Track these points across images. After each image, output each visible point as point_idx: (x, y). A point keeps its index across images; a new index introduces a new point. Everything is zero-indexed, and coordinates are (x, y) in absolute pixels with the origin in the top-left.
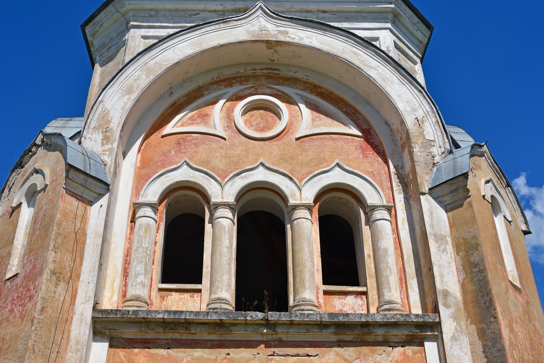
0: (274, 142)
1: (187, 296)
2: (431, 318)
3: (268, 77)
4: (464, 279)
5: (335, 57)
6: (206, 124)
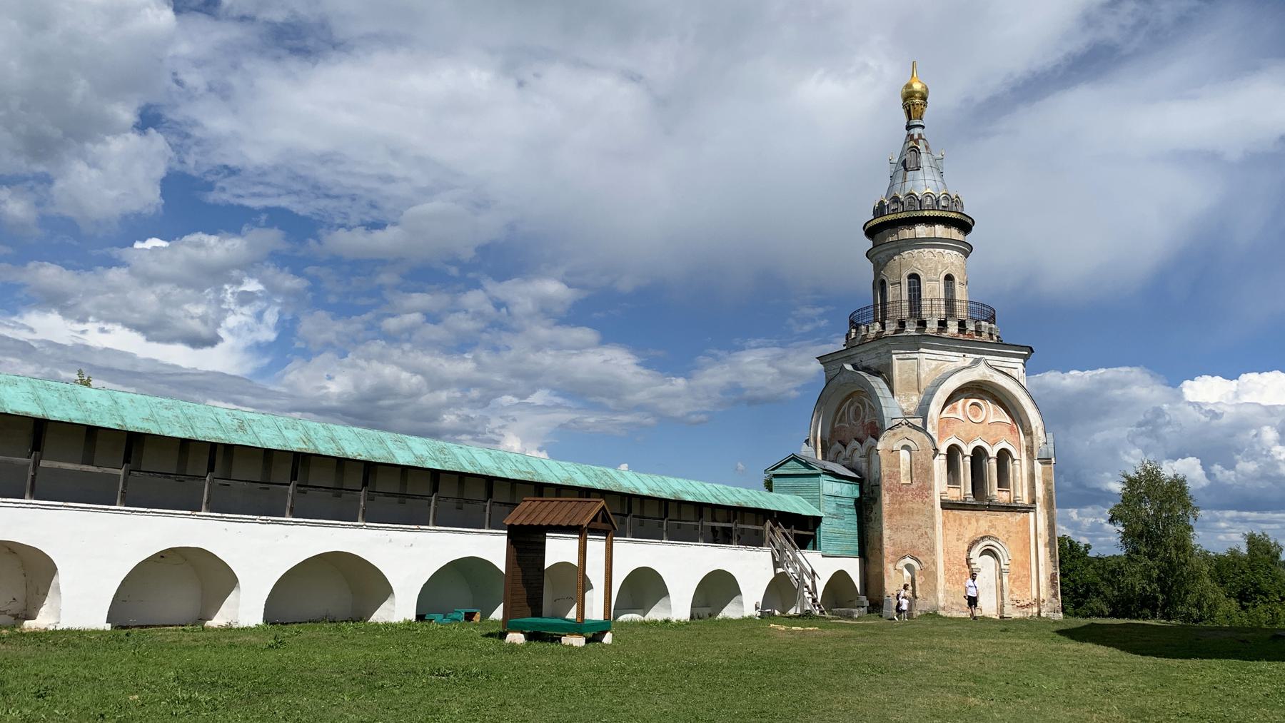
0: (981, 425)
1: (955, 489)
2: (1034, 506)
5: (1014, 397)
6: (956, 413)
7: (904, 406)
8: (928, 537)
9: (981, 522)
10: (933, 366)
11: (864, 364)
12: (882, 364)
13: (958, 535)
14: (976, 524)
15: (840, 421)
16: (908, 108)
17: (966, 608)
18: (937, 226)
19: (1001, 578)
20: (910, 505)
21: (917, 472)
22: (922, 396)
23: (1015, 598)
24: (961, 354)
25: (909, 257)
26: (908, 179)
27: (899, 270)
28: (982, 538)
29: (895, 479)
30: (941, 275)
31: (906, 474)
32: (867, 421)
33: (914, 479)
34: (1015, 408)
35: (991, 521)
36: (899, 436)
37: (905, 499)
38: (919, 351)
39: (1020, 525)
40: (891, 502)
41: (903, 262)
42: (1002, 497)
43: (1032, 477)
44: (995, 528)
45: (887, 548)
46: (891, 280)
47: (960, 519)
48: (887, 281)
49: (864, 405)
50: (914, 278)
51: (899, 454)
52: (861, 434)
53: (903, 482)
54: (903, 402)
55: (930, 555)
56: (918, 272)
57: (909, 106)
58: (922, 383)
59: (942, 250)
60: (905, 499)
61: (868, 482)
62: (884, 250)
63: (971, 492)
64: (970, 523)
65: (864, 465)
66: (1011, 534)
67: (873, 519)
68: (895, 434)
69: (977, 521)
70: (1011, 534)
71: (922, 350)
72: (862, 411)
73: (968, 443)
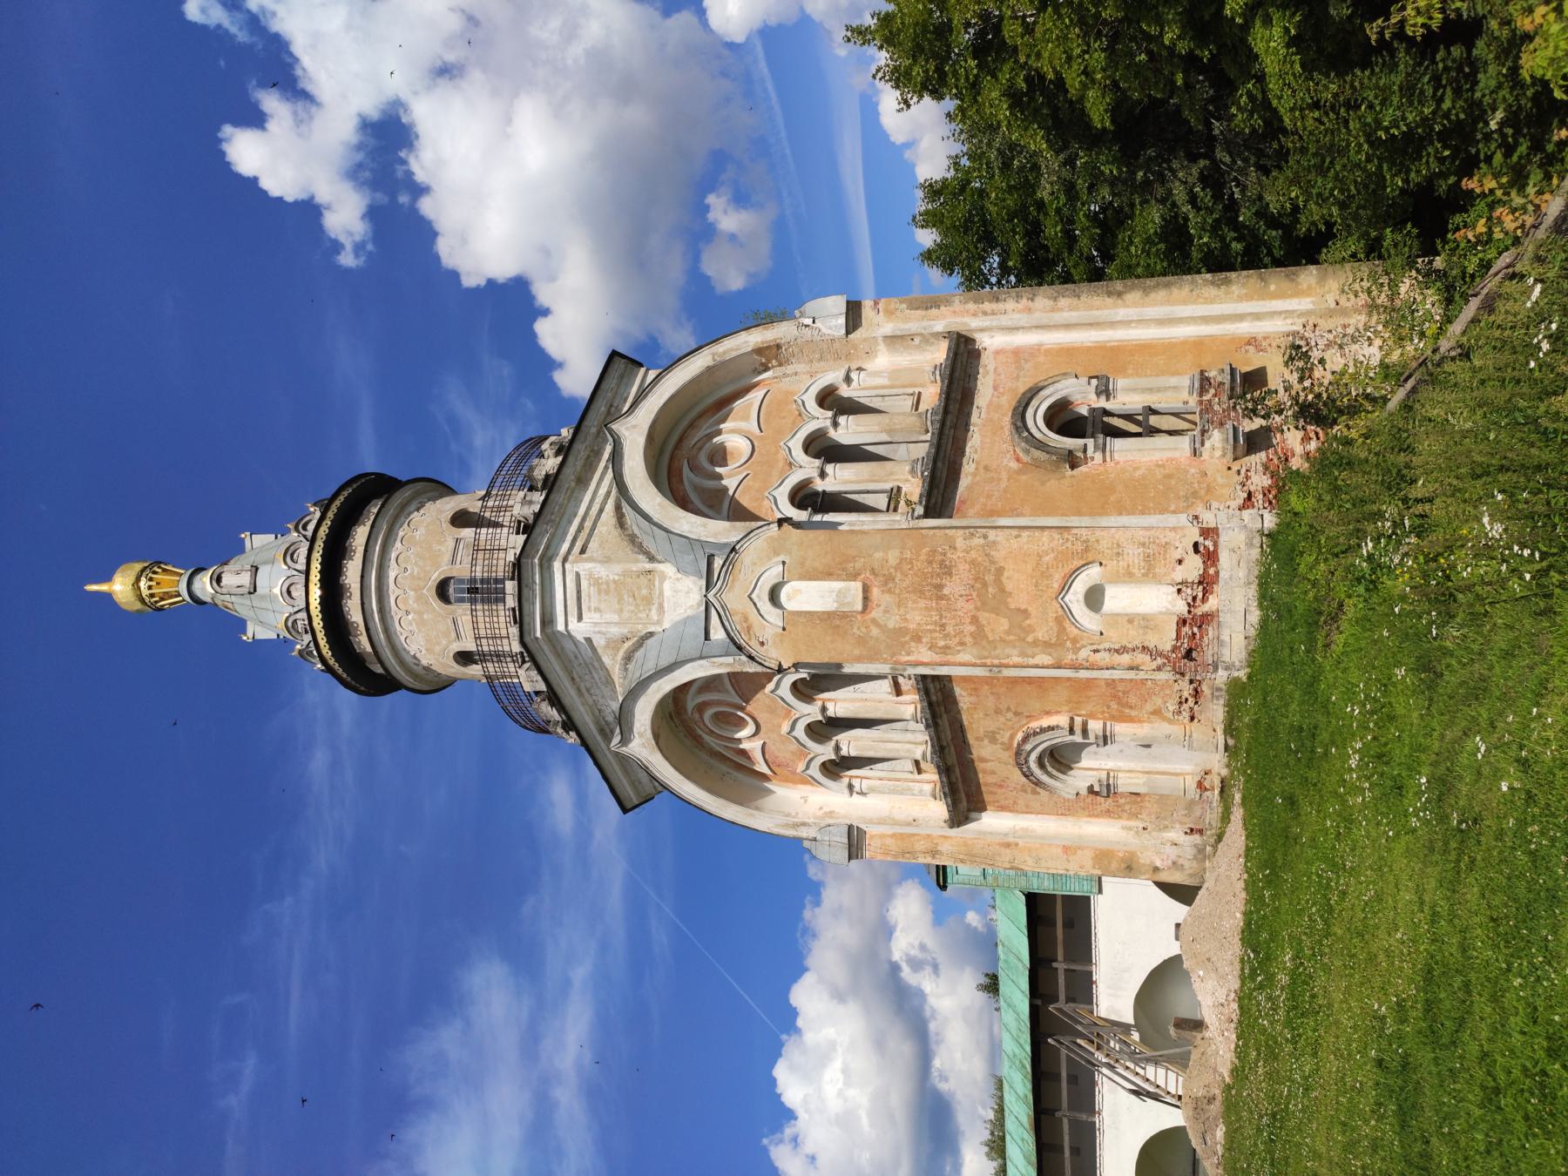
14: (989, 764)
23: (1172, 706)
39: (976, 690)
44: (993, 732)
64: (994, 773)
66: (1003, 706)
69: (983, 760)
70: (1003, 706)
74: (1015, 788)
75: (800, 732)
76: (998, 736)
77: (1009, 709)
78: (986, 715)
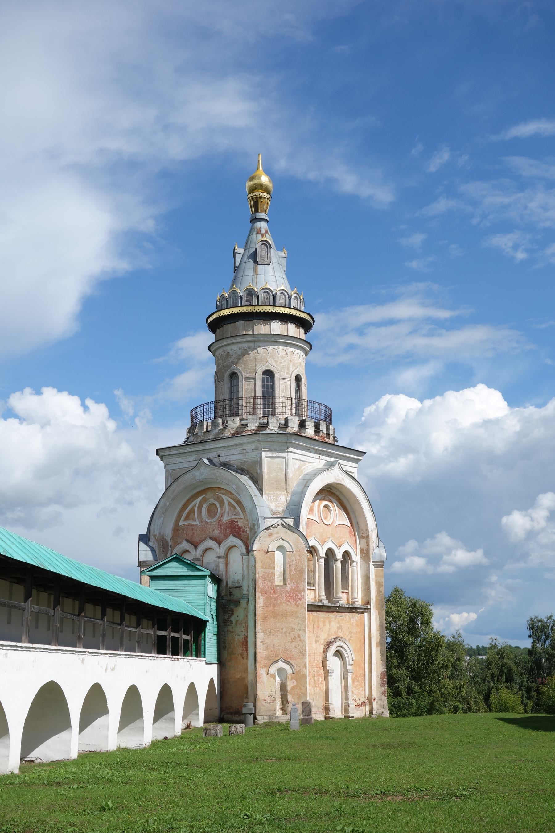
3: (328, 491)
4: (377, 595)
6: (313, 514)
7: (273, 506)
8: (300, 640)
9: (333, 623)
10: (297, 467)
11: (223, 459)
12: (247, 461)
13: (317, 637)
14: (328, 624)
15: (187, 518)
16: (255, 200)
17: (321, 710)
18: (289, 324)
19: (345, 678)
20: (283, 607)
21: (292, 573)
22: (289, 496)
24: (317, 456)
25: (265, 353)
26: (259, 272)
27: (254, 365)
28: (335, 639)
29: (270, 581)
30: (293, 374)
31: (279, 576)
32: (225, 519)
33: (289, 581)
34: (354, 512)
35: (339, 623)
36: (275, 536)
37: (279, 602)
38: (289, 450)
39: (358, 626)
40: (265, 605)
41: (258, 357)
42: (343, 599)
43: (367, 579)
44: (342, 629)
45: (260, 652)
46: (245, 375)
47: (318, 621)
48: (239, 374)
49: (222, 503)
50: (269, 374)
51: (274, 555)
52: (216, 532)
53: (277, 583)
54: (271, 502)
55: (302, 658)
56: (272, 369)
57: (257, 198)
58: (290, 483)
59: (293, 349)
60: (279, 602)
61: (225, 585)
62: (237, 343)
63: (324, 594)
65: (222, 566)
67: (234, 622)
68: (270, 535)
69: (330, 622)
71: (291, 449)
72: (219, 509)
73: (323, 545)
74: (317, 633)
75: (329, 545)
76: (340, 631)
77: (351, 637)
78: (349, 628)
